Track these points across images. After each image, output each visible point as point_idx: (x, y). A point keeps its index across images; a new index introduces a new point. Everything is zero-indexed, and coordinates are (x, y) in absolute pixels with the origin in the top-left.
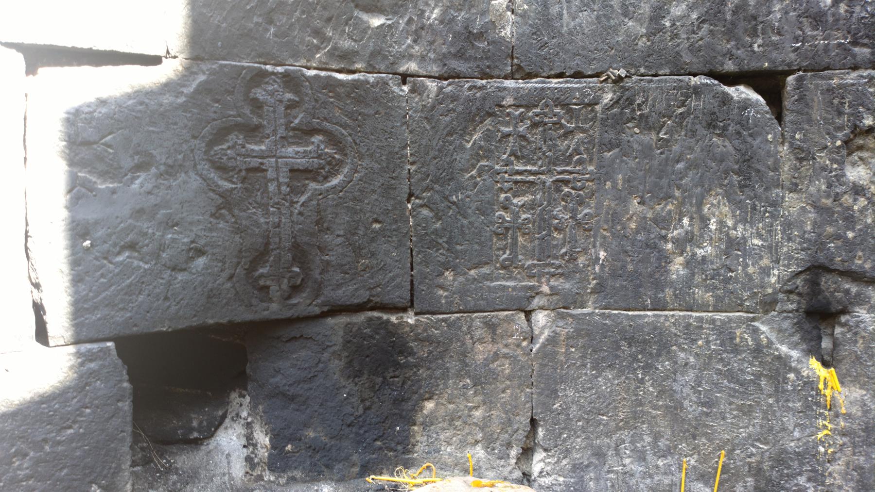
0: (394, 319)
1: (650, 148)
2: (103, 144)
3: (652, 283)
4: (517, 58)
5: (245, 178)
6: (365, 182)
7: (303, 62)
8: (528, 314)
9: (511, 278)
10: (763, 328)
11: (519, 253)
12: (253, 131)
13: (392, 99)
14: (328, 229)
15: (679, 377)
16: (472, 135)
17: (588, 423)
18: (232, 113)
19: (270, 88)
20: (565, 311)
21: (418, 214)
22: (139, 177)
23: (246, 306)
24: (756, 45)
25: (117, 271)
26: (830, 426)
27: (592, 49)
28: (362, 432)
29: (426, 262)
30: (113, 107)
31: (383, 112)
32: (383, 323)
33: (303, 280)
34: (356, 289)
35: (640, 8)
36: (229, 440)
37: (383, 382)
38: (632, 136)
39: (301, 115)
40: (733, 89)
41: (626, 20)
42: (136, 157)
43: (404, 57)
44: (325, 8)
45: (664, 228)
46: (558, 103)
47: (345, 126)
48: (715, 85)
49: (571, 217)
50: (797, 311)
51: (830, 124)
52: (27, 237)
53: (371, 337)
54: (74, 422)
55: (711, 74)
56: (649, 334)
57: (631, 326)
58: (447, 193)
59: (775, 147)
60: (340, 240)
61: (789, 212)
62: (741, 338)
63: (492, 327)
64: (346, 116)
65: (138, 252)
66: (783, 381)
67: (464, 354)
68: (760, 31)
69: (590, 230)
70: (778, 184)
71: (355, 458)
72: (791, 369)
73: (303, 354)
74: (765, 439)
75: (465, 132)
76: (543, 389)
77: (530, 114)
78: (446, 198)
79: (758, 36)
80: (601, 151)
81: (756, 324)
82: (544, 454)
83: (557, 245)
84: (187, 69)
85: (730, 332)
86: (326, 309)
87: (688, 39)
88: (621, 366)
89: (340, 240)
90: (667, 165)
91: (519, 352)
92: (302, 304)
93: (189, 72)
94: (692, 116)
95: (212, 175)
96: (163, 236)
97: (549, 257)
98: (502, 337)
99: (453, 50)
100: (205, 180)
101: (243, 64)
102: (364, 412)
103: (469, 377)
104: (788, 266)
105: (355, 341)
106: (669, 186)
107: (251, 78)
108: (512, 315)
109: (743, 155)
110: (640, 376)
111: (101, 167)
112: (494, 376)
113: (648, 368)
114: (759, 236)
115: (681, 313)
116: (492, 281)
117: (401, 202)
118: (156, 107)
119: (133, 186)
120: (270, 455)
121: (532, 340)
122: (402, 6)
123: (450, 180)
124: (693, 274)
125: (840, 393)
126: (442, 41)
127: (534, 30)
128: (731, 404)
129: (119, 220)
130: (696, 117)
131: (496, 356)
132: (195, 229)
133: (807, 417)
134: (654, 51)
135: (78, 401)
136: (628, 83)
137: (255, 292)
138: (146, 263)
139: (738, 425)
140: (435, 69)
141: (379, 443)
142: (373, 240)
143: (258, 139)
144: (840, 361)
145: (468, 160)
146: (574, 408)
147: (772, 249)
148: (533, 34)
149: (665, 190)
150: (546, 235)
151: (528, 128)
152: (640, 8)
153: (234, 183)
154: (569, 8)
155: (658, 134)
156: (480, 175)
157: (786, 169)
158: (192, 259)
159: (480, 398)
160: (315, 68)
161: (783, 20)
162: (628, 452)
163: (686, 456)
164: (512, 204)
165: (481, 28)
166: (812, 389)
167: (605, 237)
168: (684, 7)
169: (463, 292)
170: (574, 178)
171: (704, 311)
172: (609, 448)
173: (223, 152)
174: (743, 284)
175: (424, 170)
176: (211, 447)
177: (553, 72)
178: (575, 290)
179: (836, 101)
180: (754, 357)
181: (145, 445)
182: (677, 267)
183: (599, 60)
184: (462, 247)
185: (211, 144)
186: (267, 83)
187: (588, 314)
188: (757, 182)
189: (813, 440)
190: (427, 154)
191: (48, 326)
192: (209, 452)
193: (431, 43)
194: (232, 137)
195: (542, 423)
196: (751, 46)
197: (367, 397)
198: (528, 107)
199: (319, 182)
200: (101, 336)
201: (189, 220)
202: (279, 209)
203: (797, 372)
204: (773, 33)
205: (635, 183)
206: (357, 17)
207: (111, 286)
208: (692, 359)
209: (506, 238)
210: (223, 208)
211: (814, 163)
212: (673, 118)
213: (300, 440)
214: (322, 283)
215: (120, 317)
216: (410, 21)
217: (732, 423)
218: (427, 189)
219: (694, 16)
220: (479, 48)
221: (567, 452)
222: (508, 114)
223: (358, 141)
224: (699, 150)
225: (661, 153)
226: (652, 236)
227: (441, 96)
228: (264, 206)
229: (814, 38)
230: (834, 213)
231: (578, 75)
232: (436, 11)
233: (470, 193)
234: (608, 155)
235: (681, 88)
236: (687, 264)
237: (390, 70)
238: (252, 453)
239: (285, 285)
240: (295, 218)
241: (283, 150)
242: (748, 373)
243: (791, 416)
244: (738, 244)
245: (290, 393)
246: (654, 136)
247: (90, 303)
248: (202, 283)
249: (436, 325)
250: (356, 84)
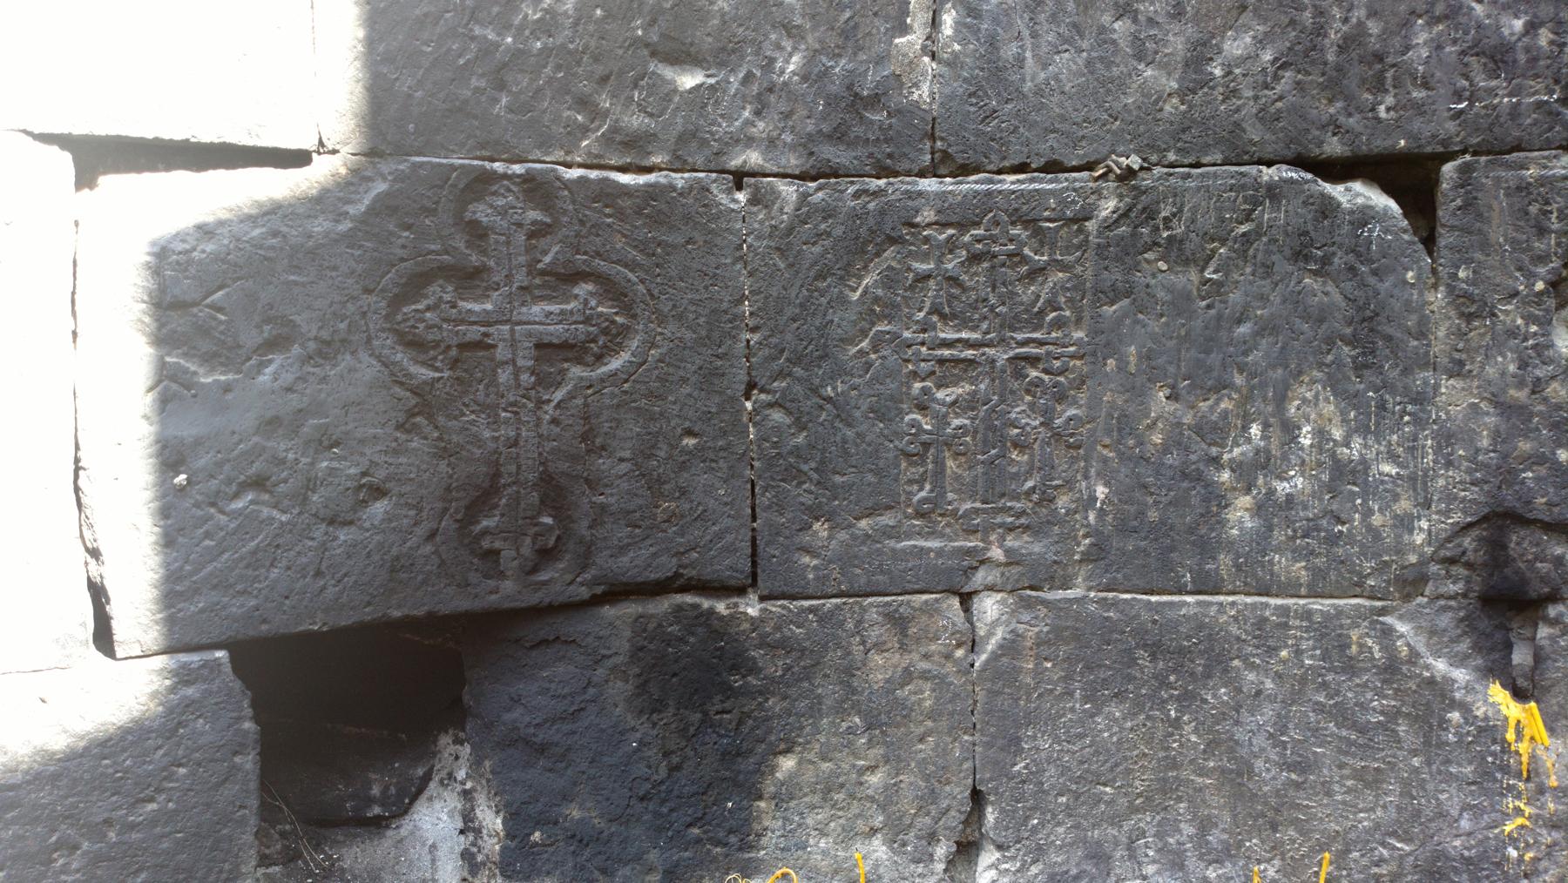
0: (721, 607)
1: (1188, 297)
2: (208, 306)
3: (1193, 543)
4: (942, 139)
7: (559, 155)
8: (966, 599)
9: (933, 534)
10: (1402, 628)
11: (949, 488)
12: (469, 278)
13: (717, 218)
14: (603, 448)
15: (1245, 716)
16: (860, 278)
17: (1077, 799)
18: (433, 247)
19: (500, 202)
20: (1033, 593)
21: (763, 419)
22: (270, 361)
23: (459, 586)
24: (1382, 108)
26: (1528, 810)
27: (1079, 120)
28: (665, 810)
29: (779, 506)
30: (226, 242)
31: (700, 239)
32: (702, 615)
33: (559, 538)
35: (1166, 43)
36: (435, 820)
37: (703, 721)
38: (1154, 276)
39: (556, 249)
40: (1340, 188)
41: (1141, 66)
42: (267, 328)
43: (738, 141)
44: (596, 59)
45: (1215, 444)
46: (1017, 218)
47: (632, 266)
48: (1307, 182)
50: (1465, 595)
51: (1524, 251)
52: (77, 469)
53: (681, 640)
54: (159, 790)
55: (1299, 162)
56: (1188, 638)
57: (1155, 622)
58: (817, 381)
59: (1421, 294)
60: (624, 467)
61: (1447, 413)
62: (1361, 646)
65: (271, 492)
66: (1440, 726)
67: (849, 671)
68: (1389, 81)
69: (1079, 447)
70: (1428, 363)
71: (653, 856)
72: (1454, 705)
73: (560, 672)
74: (1406, 832)
75: (848, 273)
76: (994, 737)
77: (967, 238)
78: (815, 391)
79: (1386, 91)
80: (1096, 303)
81: (1388, 620)
82: (998, 855)
83: (1017, 474)
84: (354, 171)
85: (1340, 635)
86: (599, 590)
87: (1256, 98)
88: (1138, 696)
89: (624, 467)
90: (1218, 327)
91: (950, 668)
92: (558, 581)
93: (356, 178)
94: (1265, 239)
95: (399, 356)
96: (312, 464)
97: (1003, 495)
98: (918, 640)
99: (826, 128)
100: (386, 366)
102: (669, 776)
103: (859, 713)
104: (1446, 513)
105: (652, 647)
106: (1224, 366)
107: (467, 186)
108: (937, 600)
109: (1359, 309)
111: (205, 346)
112: (905, 712)
113: (1187, 699)
114: (1393, 457)
115: (1249, 600)
116: (899, 538)
117: (733, 399)
119: (261, 378)
120: (503, 849)
121: (973, 647)
122: (733, 51)
123: (821, 358)
124: (1270, 528)
125: (1547, 749)
126: (805, 113)
127: (972, 89)
128: (1341, 766)
129: (236, 438)
130: (1274, 241)
131: (908, 676)
132: (368, 451)
133: (1486, 792)
134: (1194, 121)
135: (164, 755)
136: (1146, 181)
137: (475, 561)
139: (1355, 806)
140: (793, 162)
141: (696, 831)
142: (683, 467)
144: (1547, 689)
145: (855, 323)
146: (1052, 771)
147: (1417, 482)
148: (970, 96)
149: (1215, 374)
150: (998, 457)
151: (962, 263)
152: (1166, 43)
153: (437, 369)
154: (1035, 47)
155: (1202, 270)
156: (875, 349)
157: (1441, 333)
159: (878, 751)
160: (580, 166)
161: (1433, 61)
162: (1151, 853)
163: (1259, 862)
165: (876, 87)
166: (1494, 742)
167: (1105, 460)
168: (1248, 40)
169: (847, 560)
170: (1048, 353)
171: (1292, 596)
172: (1117, 844)
174: (1362, 546)
175: (774, 340)
176: (403, 832)
177: (1007, 164)
178: (1051, 557)
179: (1534, 209)
180: (1384, 682)
181: (288, 827)
182: (1240, 514)
183: (1092, 139)
184: (845, 479)
185: (397, 302)
186: (494, 193)
187: (1076, 600)
188: (1387, 358)
189: (1496, 837)
190: (780, 312)
191: (114, 623)
192: (401, 841)
193: (787, 116)
194: (434, 289)
195: (992, 798)
196: (1373, 110)
197: (674, 747)
198: (963, 227)
200: (204, 641)
201: (358, 435)
202: (516, 413)
203: (1465, 708)
204: (1414, 84)
206: (653, 73)
208: (1269, 684)
209: (923, 463)
210: (418, 414)
211: (1493, 323)
212: (1230, 243)
213: (556, 823)
214: (592, 543)
215: (237, 607)
216: (748, 78)
217: (1344, 803)
218: (781, 375)
219: (1267, 56)
220: (872, 122)
221: (1039, 853)
222: (927, 240)
223: (656, 292)
224: (1278, 300)
225: (1209, 307)
226: (1193, 457)
228: (489, 409)
229: (1492, 92)
230: (1532, 415)
231: (1053, 167)
232: (794, 59)
234: (1109, 310)
235: (1243, 187)
236: (1258, 510)
237: (712, 166)
238: (474, 844)
239: (526, 550)
240: (544, 429)
241: (524, 309)
242: (1374, 709)
243: (1454, 792)
244: (1353, 472)
245: (537, 740)
246: (1194, 276)
247: (187, 583)
248: (381, 545)
249: (799, 619)
250: (651, 192)
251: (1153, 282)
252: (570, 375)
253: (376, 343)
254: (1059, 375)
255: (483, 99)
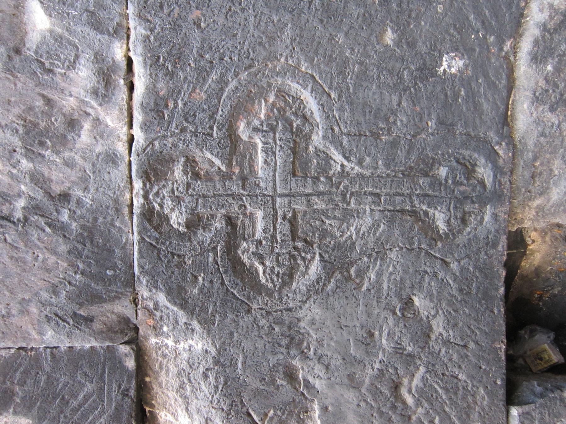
5: (305, 241)
6: (317, 54)
14: (387, 120)
18: (211, 259)
19: (168, 203)
25: (426, 405)
32: (543, 37)
34: (486, 76)
39: (209, 155)
42: (279, 382)
47: (222, 82)
64: (204, 79)
100: (308, 299)
101: (135, 242)
118: (210, 359)
129: (363, 404)
132: (376, 311)
138: (418, 369)
143: (247, 222)
153: (313, 258)
158: (416, 313)
173: (268, 271)
194: (245, 259)
199: (312, 131)
201: (364, 317)
202: (352, 194)
207: (444, 411)
210: (348, 272)
241: (262, 184)
248: (450, 303)
252: (321, 148)
253: (291, 305)
255: (78, 212)
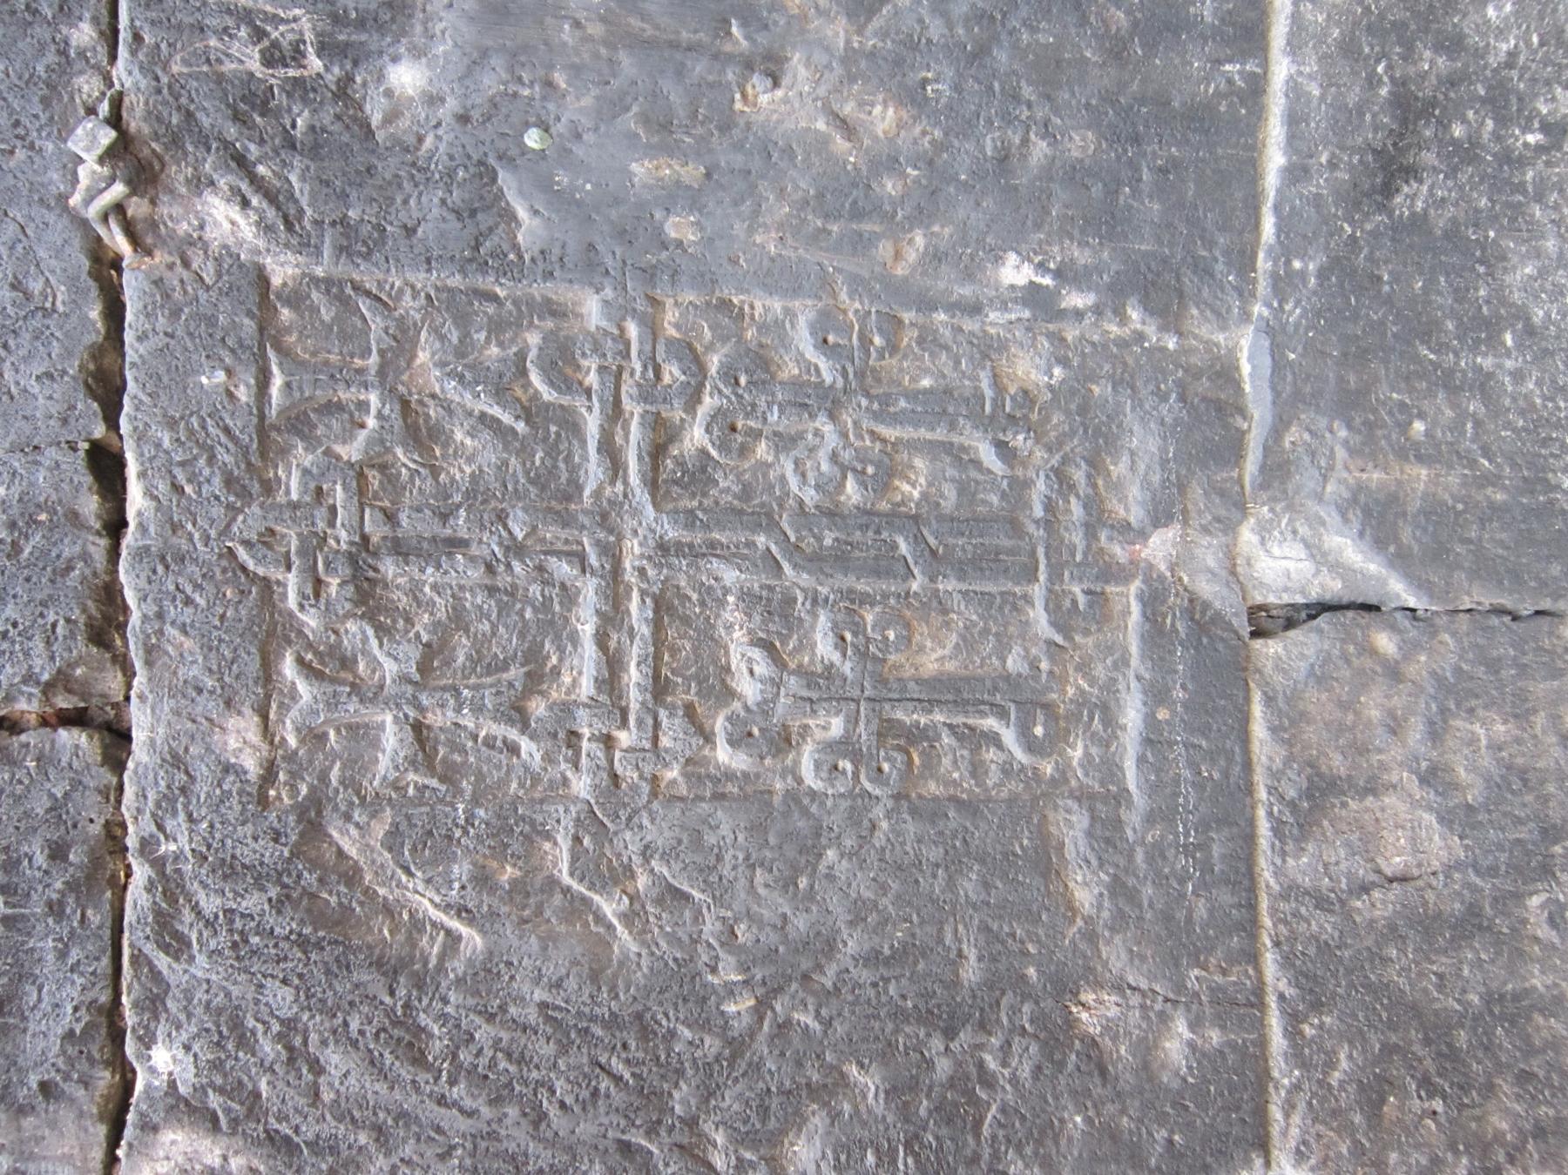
16: (418, 924)
46: (251, 480)
49: (833, 417)
56: (1372, 82)
63: (1316, 799)
77: (311, 621)
80: (509, 264)
83: (963, 489)
103: (1519, 897)
108: (1269, 700)
110: (1531, 139)
131: (1433, 776)
150: (919, 539)
151: (381, 630)
164: (765, 708)
167: (935, 257)
169: (1177, 944)
170: (645, 396)
177: (90, 505)
178: (1171, 408)
187: (1276, 352)
198: (272, 632)
205: (676, 96)
226: (936, 29)
227: (214, 1101)
233: (710, 927)
234: (530, 228)
251: (452, 104)
254: (702, 369)
